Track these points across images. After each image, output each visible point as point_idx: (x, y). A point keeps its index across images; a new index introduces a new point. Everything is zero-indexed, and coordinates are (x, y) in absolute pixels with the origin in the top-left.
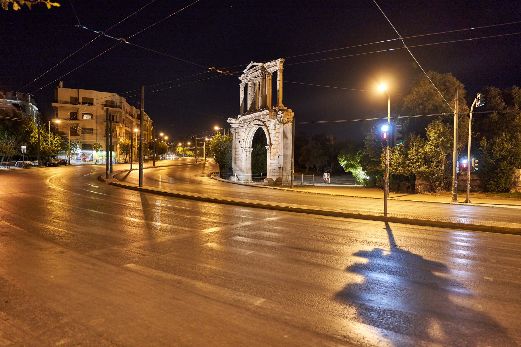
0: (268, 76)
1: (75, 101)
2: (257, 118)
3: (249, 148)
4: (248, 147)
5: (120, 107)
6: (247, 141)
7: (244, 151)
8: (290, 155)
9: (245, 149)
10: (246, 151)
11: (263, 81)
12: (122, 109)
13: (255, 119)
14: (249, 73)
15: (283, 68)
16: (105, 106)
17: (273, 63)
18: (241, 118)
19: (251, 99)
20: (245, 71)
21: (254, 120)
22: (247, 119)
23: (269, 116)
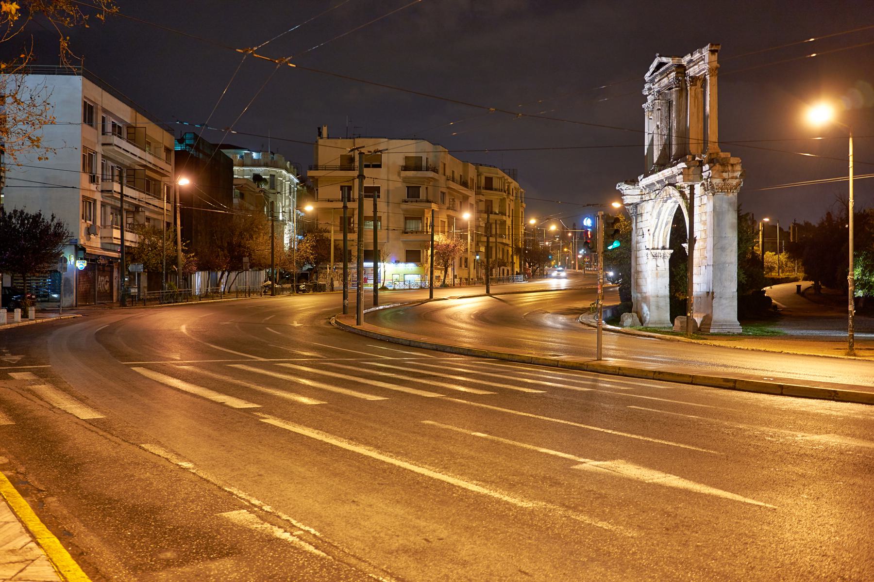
0: (691, 85)
1: (347, 163)
2: (672, 181)
3: (664, 248)
4: (660, 247)
5: (435, 170)
6: (656, 234)
7: (650, 257)
8: (731, 263)
9: (652, 251)
10: (655, 256)
11: (679, 97)
12: (437, 172)
13: (667, 182)
14: (656, 81)
15: (719, 65)
16: (406, 168)
17: (697, 55)
18: (644, 182)
19: (661, 139)
20: (647, 76)
21: (665, 186)
22: (653, 184)
23: (681, 176)
